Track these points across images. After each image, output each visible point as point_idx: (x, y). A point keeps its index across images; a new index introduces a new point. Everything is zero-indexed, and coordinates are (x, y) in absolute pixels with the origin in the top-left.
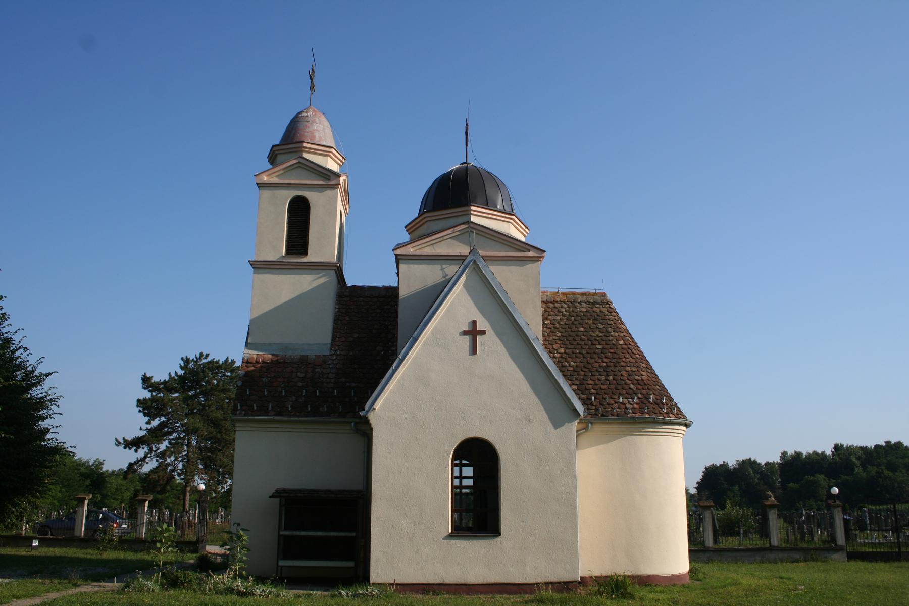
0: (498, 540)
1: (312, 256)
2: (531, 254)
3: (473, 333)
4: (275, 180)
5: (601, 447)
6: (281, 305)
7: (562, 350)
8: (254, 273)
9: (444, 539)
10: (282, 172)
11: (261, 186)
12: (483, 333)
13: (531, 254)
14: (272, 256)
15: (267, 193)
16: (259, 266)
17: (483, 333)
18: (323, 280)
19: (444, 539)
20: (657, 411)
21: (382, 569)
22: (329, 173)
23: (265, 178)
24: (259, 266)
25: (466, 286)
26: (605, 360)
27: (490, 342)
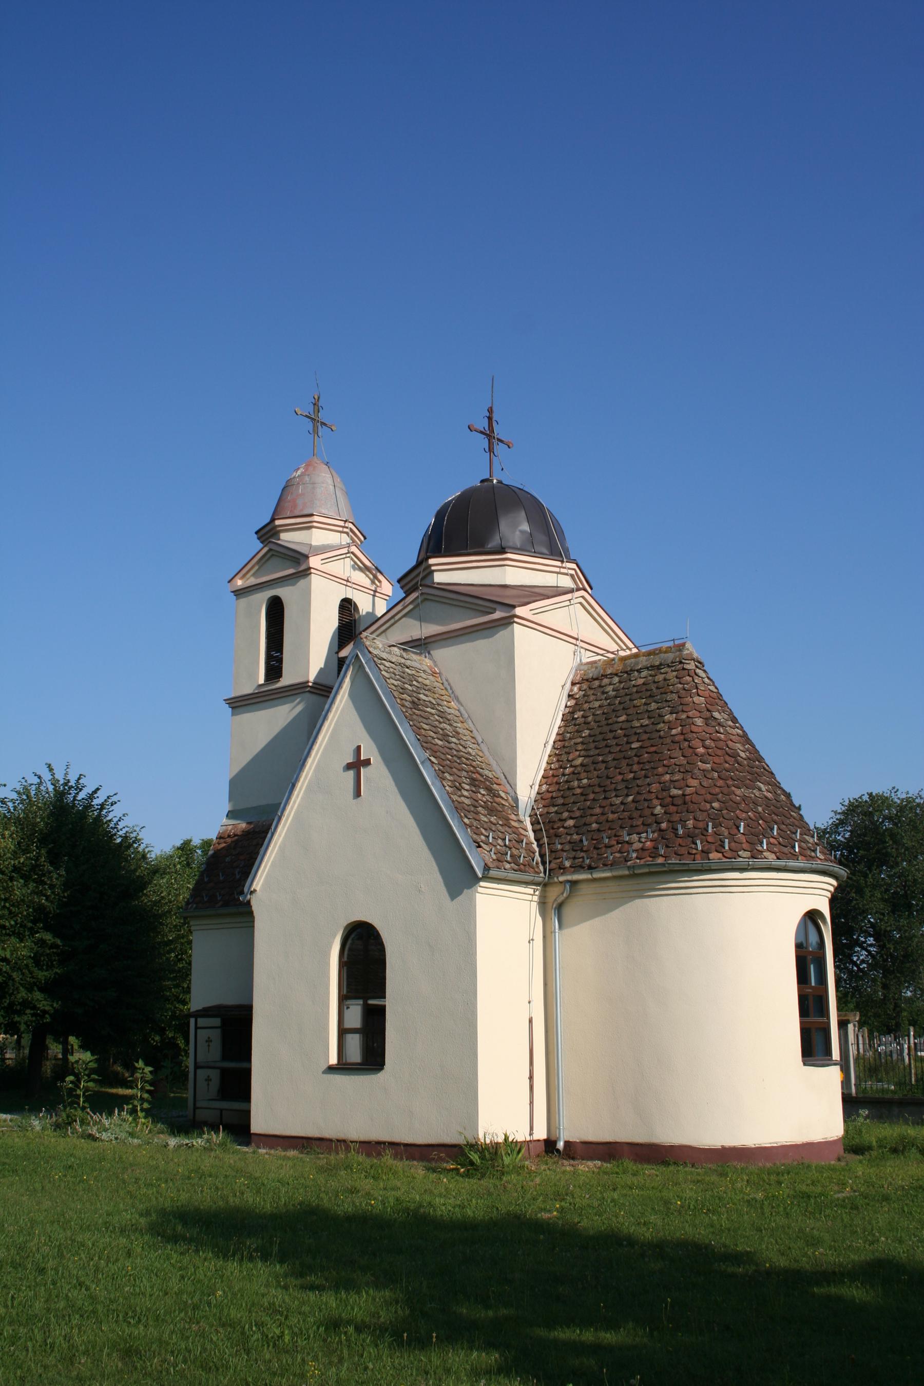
0: (381, 1075)
1: (287, 679)
2: (498, 615)
3: (357, 764)
4: (252, 581)
5: (597, 922)
6: (257, 755)
7: (579, 761)
8: (233, 715)
9: (324, 1072)
10: (257, 567)
11: (239, 593)
12: (367, 762)
13: (498, 615)
14: (248, 689)
15: (243, 601)
16: (239, 704)
17: (367, 762)
18: (299, 708)
19: (324, 1072)
20: (683, 851)
21: (264, 1116)
22: (298, 556)
23: (239, 583)
24: (239, 704)
25: (352, 695)
26: (636, 767)
27: (377, 775)
